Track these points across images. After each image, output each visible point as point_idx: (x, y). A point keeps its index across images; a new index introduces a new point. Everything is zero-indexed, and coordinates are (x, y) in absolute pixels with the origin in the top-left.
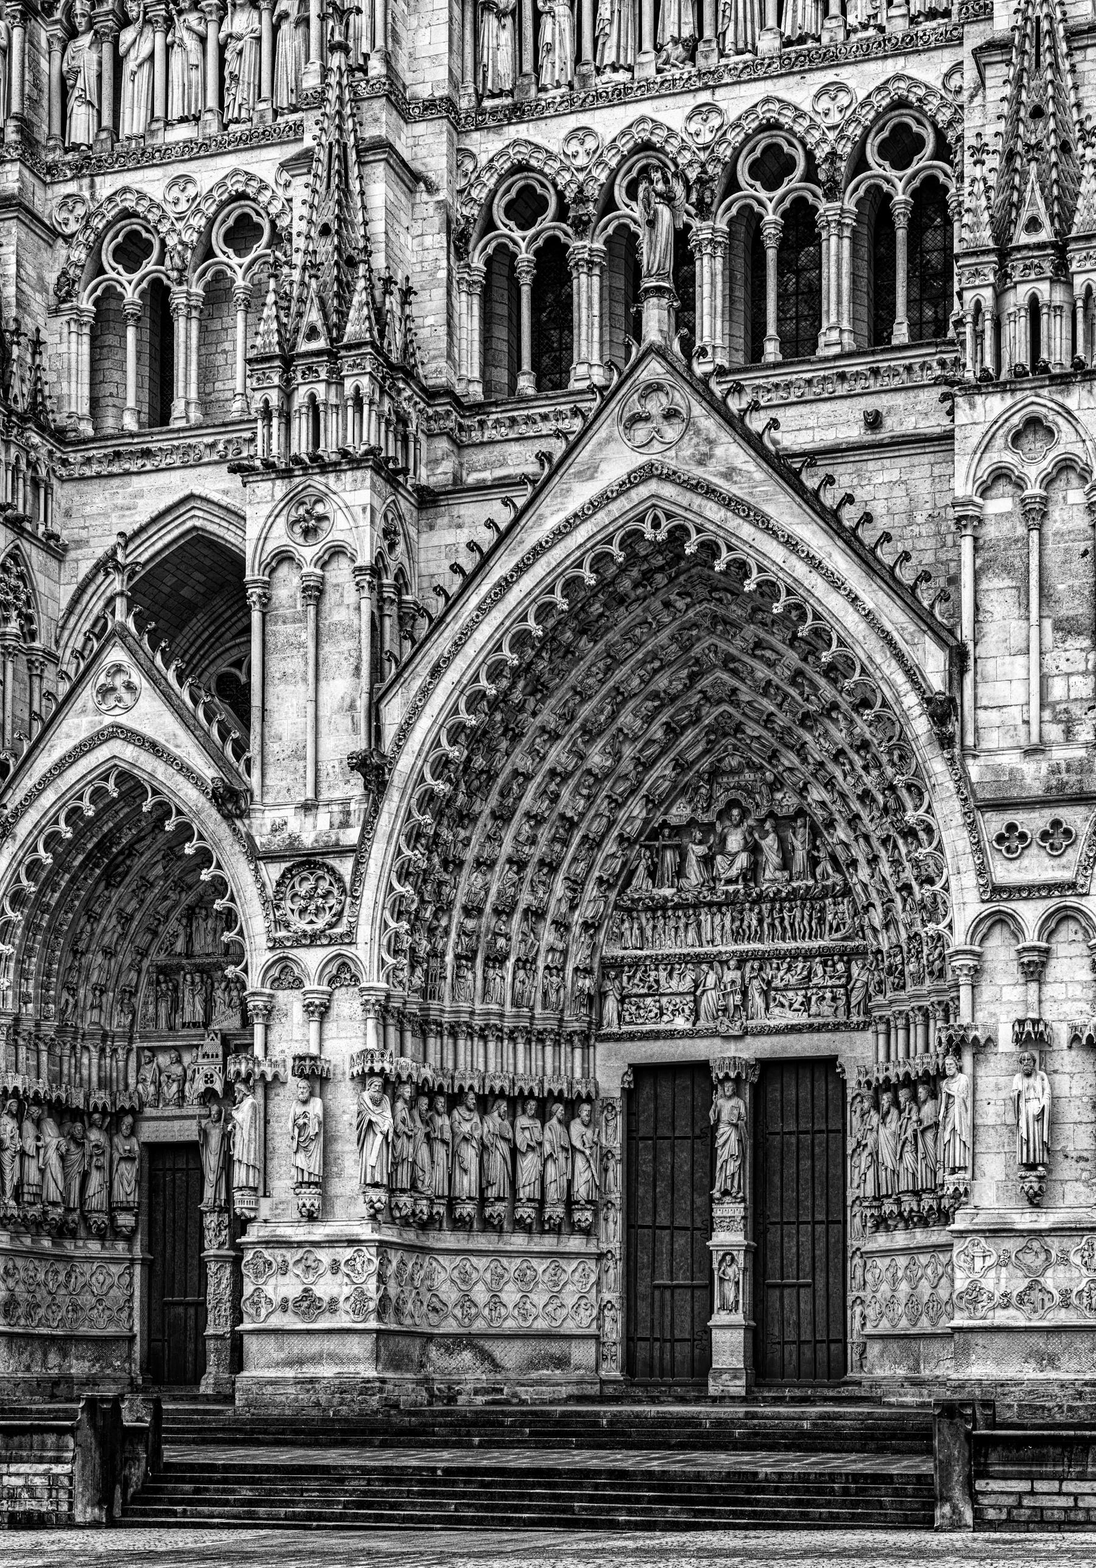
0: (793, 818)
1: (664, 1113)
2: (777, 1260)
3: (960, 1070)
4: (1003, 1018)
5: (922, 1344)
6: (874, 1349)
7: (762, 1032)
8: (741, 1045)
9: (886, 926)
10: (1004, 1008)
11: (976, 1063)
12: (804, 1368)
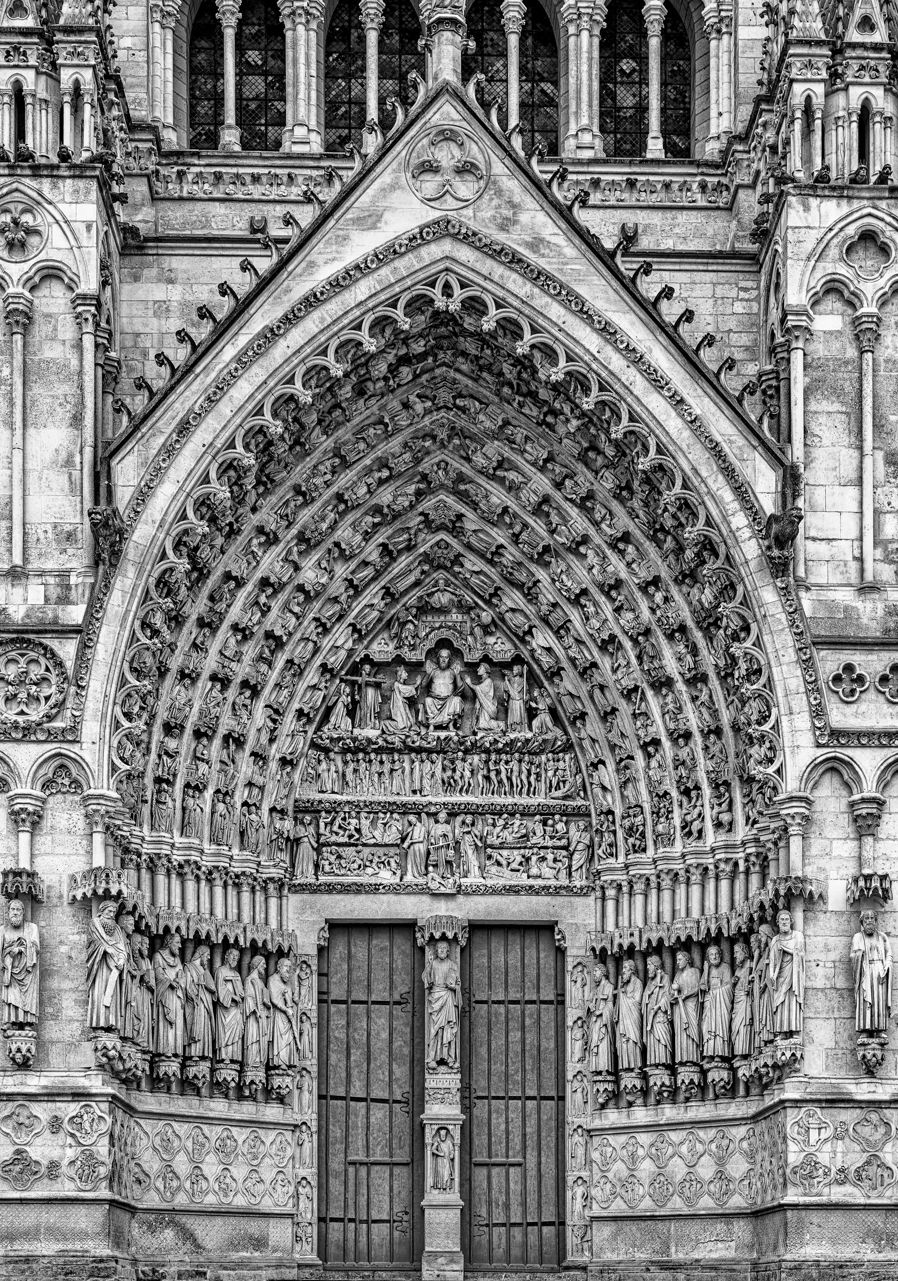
0: (508, 665)
1: (360, 974)
2: (485, 1137)
3: (792, 927)
4: (833, 874)
5: (673, 1226)
6: (602, 1233)
7: (476, 891)
8: (452, 904)
9: (624, 785)
10: (835, 863)
11: (806, 919)
12: (516, 1252)
